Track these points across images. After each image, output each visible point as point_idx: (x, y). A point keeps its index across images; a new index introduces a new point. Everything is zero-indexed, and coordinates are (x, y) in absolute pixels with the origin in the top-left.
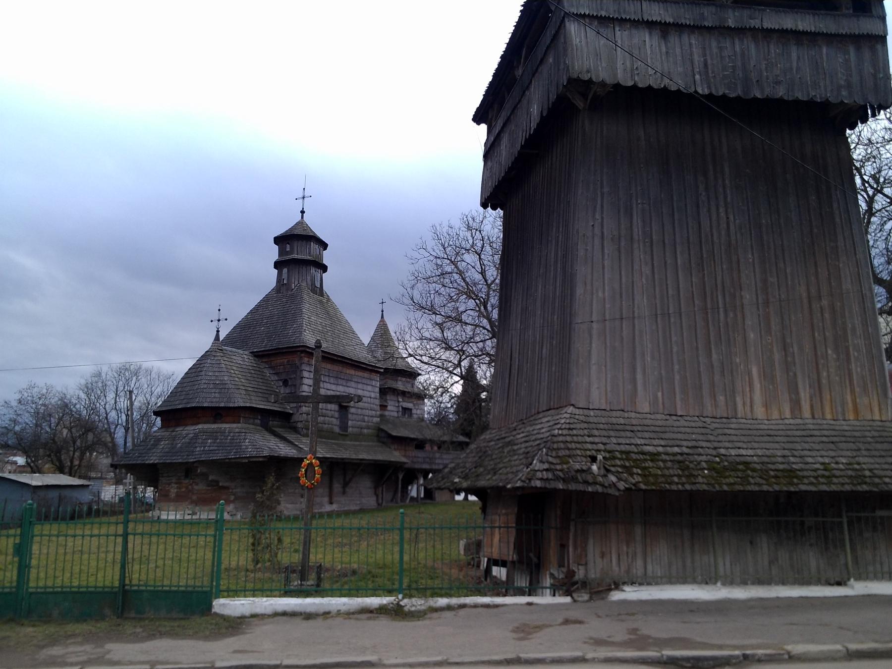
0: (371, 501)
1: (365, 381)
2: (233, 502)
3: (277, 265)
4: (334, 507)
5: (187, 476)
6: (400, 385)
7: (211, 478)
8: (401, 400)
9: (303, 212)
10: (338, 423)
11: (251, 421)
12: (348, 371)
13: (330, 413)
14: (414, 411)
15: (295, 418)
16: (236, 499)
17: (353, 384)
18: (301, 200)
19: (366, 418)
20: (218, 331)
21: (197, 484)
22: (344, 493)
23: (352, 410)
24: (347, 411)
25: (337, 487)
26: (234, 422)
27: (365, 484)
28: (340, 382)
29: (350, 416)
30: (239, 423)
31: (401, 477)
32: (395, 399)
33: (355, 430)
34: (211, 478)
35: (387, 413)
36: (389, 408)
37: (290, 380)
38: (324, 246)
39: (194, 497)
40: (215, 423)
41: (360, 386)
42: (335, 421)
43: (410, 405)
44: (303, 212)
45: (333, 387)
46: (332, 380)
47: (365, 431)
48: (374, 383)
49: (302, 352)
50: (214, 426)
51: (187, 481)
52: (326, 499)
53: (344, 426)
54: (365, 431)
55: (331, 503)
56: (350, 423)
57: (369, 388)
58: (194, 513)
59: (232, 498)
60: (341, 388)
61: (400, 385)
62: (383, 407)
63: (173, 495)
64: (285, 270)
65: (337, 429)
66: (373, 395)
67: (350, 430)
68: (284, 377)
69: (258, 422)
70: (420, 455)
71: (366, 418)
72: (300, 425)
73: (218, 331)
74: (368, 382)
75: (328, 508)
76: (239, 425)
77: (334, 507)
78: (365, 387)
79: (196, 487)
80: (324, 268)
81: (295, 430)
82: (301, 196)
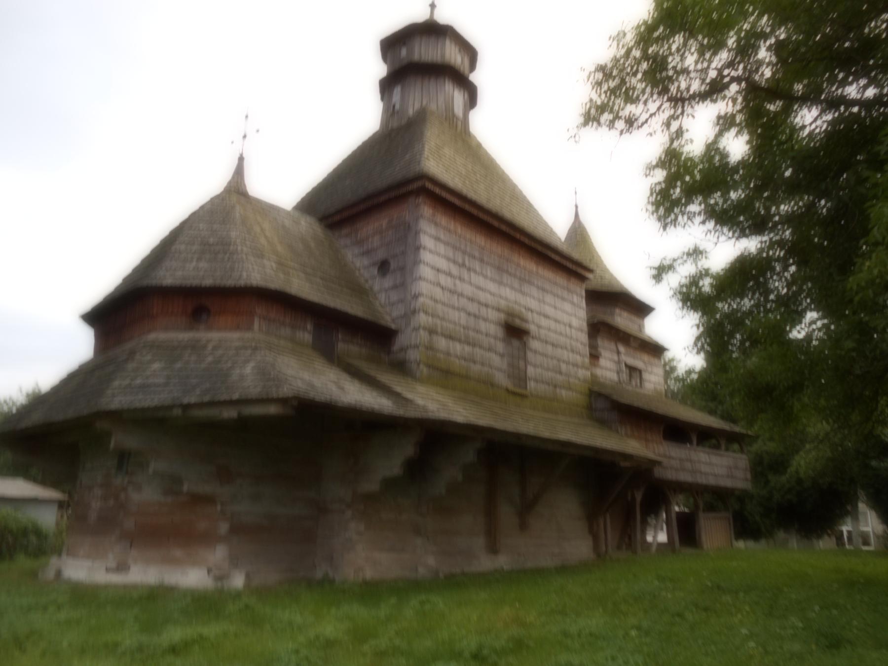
0: (580, 548)
1: (559, 292)
3: (387, 86)
4: (503, 561)
6: (622, 319)
8: (622, 349)
9: (433, 6)
10: (505, 366)
11: (286, 331)
12: (522, 262)
13: (486, 341)
14: (646, 376)
15: (402, 340)
17: (534, 291)
19: (564, 367)
20: (241, 159)
22: (523, 526)
23: (534, 344)
24: (525, 345)
25: (506, 513)
26: (238, 328)
27: (564, 508)
28: (506, 278)
29: (530, 355)
30: (249, 328)
31: (639, 497)
32: (612, 346)
33: (542, 388)
35: (599, 372)
36: (602, 362)
37: (395, 264)
38: (471, 53)
39: (129, 524)
41: (549, 298)
42: (496, 360)
43: (638, 363)
44: (433, 6)
45: (492, 286)
46: (489, 271)
48: (575, 299)
50: (185, 336)
52: (480, 542)
54: (564, 393)
55: (493, 549)
56: (531, 371)
57: (567, 307)
58: (122, 567)
59: (224, 528)
60: (507, 292)
61: (622, 319)
62: (595, 356)
63: (93, 516)
64: (397, 91)
65: (502, 379)
66: (575, 322)
67: (531, 385)
68: (381, 255)
70: (673, 454)
72: (413, 355)
73: (241, 159)
74: (565, 294)
75: (485, 563)
76: (248, 335)
77: (503, 561)
78: (559, 303)
80: (471, 94)
81: (401, 367)
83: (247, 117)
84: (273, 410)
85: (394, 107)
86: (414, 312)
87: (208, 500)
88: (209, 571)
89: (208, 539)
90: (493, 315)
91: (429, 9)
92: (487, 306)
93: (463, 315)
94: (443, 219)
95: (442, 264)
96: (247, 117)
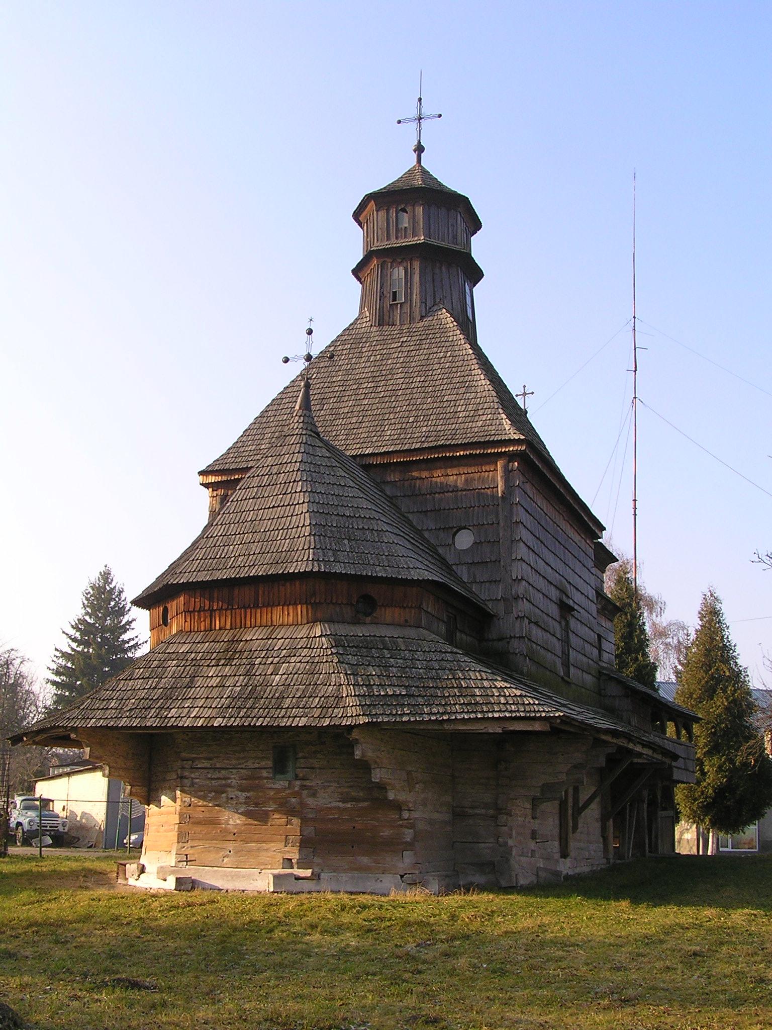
2: (409, 846)
5: (280, 768)
7: (377, 776)
9: (420, 149)
16: (415, 838)
18: (414, 125)
21: (314, 795)
22: (575, 827)
23: (572, 622)
26: (405, 624)
34: (377, 776)
40: (356, 622)
44: (420, 149)
47: (586, 676)
49: (511, 457)
51: (281, 784)
53: (566, 664)
55: (564, 855)
59: (408, 835)
67: (572, 669)
69: (443, 628)
71: (586, 645)
72: (515, 645)
79: (310, 801)
82: (414, 113)
83: (310, 332)
84: (537, 727)
85: (395, 293)
86: (517, 598)
87: (398, 807)
88: (402, 876)
89: (395, 846)
90: (554, 593)
91: (415, 156)
92: (551, 583)
93: (541, 595)
94: (528, 487)
95: (531, 540)
96: (310, 332)
